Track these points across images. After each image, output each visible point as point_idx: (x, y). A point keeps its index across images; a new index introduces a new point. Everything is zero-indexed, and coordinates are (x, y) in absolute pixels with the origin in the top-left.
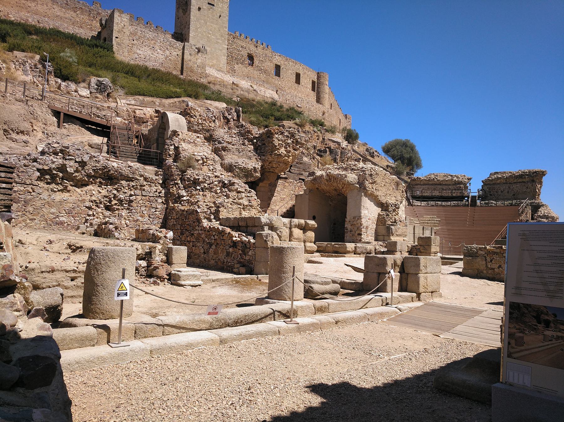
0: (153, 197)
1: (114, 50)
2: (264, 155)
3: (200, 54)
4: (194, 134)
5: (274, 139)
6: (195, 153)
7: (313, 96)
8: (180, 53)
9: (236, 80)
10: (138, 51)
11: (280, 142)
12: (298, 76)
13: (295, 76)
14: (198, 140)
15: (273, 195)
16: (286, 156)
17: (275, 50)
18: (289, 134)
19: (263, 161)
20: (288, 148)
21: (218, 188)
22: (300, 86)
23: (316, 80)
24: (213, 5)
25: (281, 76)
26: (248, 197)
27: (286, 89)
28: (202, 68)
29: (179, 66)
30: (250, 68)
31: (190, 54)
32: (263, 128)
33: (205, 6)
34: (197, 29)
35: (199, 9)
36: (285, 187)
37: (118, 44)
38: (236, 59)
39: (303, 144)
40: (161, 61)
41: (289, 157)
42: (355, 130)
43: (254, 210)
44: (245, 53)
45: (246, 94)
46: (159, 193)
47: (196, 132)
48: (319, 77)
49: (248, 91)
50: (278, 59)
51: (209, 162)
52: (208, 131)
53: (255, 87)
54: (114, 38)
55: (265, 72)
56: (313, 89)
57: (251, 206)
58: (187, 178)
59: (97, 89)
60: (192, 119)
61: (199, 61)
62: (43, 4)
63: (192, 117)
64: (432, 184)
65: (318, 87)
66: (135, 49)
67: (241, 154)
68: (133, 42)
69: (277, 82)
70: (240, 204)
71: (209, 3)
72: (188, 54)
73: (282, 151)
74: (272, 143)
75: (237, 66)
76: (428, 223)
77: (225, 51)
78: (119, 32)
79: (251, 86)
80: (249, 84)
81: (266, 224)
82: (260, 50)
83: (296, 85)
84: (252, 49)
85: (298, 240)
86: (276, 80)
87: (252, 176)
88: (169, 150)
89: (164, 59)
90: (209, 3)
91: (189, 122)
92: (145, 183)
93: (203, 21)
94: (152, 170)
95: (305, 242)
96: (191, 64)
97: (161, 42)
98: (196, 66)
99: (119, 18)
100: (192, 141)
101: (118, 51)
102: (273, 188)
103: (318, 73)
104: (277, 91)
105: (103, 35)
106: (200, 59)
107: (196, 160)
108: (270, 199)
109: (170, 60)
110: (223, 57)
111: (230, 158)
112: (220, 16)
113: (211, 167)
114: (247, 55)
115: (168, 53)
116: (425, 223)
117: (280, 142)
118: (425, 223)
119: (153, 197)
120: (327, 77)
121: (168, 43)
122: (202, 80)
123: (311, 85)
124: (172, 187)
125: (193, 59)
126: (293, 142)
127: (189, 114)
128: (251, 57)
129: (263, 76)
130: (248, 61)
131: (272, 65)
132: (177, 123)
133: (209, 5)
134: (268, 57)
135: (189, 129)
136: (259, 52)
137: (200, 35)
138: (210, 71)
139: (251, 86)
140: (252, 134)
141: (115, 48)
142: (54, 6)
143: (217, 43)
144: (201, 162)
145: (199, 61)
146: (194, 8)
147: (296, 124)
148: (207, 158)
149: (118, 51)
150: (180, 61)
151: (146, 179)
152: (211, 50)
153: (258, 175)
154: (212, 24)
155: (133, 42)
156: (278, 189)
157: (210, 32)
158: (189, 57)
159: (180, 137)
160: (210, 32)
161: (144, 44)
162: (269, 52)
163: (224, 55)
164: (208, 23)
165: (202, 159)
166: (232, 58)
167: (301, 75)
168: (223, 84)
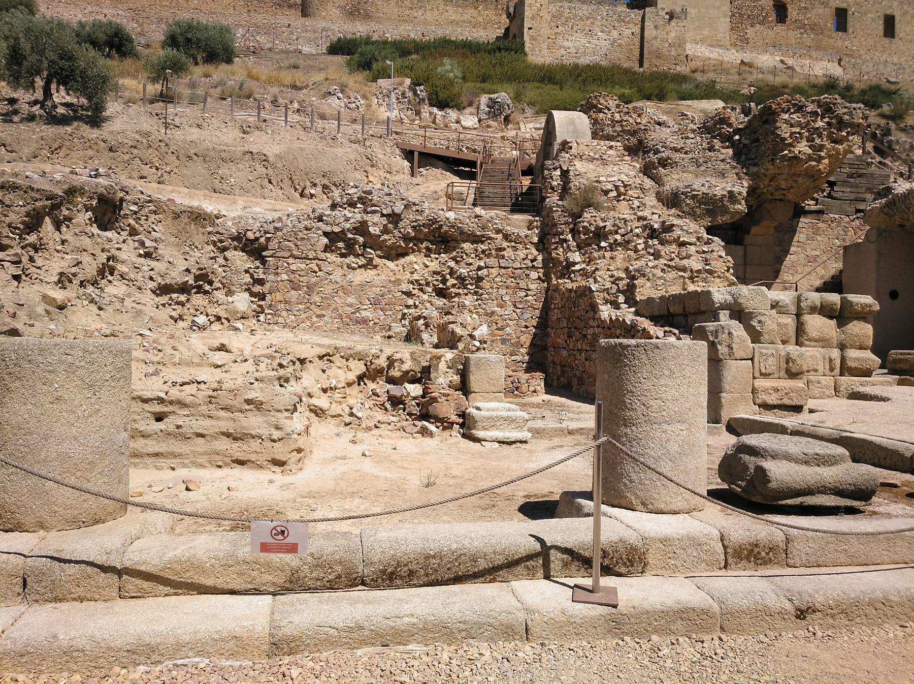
0: (521, 268)
1: (526, 49)
2: (755, 165)
3: (673, 23)
4: (602, 143)
5: (778, 124)
6: (602, 179)
8: (637, 30)
9: (747, 57)
10: (566, 44)
11: (794, 130)
13: (882, 22)
14: (610, 152)
15: (786, 252)
16: (810, 158)
18: (819, 106)
19: (754, 177)
20: (818, 141)
21: (641, 241)
22: (894, 41)
25: (850, 30)
26: (704, 252)
27: (862, 52)
28: (679, 46)
29: (637, 53)
30: (780, 28)
31: (656, 27)
36: (817, 231)
37: (533, 38)
38: (749, 17)
39: (859, 125)
40: (604, 51)
41: (819, 160)
43: (717, 280)
45: (770, 78)
46: (532, 261)
47: (609, 138)
49: (774, 71)
51: (630, 192)
52: (633, 133)
53: (790, 62)
54: (526, 30)
55: (813, 28)
57: (710, 272)
58: (584, 227)
59: (489, 112)
60: (601, 115)
61: (673, 34)
62: (432, 9)
63: (600, 111)
66: (560, 41)
67: (703, 168)
69: (839, 43)
70: (684, 269)
72: (652, 26)
73: (803, 148)
74: (773, 133)
75: (752, 29)
78: (533, 18)
79: (782, 62)
80: (778, 58)
81: (723, 307)
83: (886, 41)
85: (824, 342)
86: (840, 41)
87: (724, 210)
88: (551, 178)
89: (609, 47)
91: (595, 122)
92: (505, 244)
94: (522, 221)
95: (842, 347)
96: (656, 44)
97: (602, 18)
98: (667, 45)
100: (597, 156)
102: (786, 237)
104: (840, 61)
105: (513, 31)
106: (674, 31)
107: (602, 191)
108: (780, 260)
109: (620, 45)
110: (722, 20)
111: (674, 180)
113: (637, 203)
115: (615, 33)
117: (794, 130)
119: (521, 268)
121: (615, 17)
122: (678, 68)
124: (556, 249)
125: (661, 33)
126: (829, 124)
127: (595, 107)
129: (808, 38)
130: (773, 17)
132: (572, 127)
135: (595, 135)
138: (691, 49)
139: (782, 62)
140: (730, 125)
141: (528, 45)
142: (448, 8)
144: (614, 194)
145: (673, 34)
147: (883, 116)
148: (625, 186)
149: (533, 50)
150: (638, 44)
151: (506, 237)
153: (742, 207)
156: (800, 236)
158: (654, 32)
159: (573, 151)
161: (575, 28)
163: (725, 16)
165: (617, 187)
168: (720, 67)
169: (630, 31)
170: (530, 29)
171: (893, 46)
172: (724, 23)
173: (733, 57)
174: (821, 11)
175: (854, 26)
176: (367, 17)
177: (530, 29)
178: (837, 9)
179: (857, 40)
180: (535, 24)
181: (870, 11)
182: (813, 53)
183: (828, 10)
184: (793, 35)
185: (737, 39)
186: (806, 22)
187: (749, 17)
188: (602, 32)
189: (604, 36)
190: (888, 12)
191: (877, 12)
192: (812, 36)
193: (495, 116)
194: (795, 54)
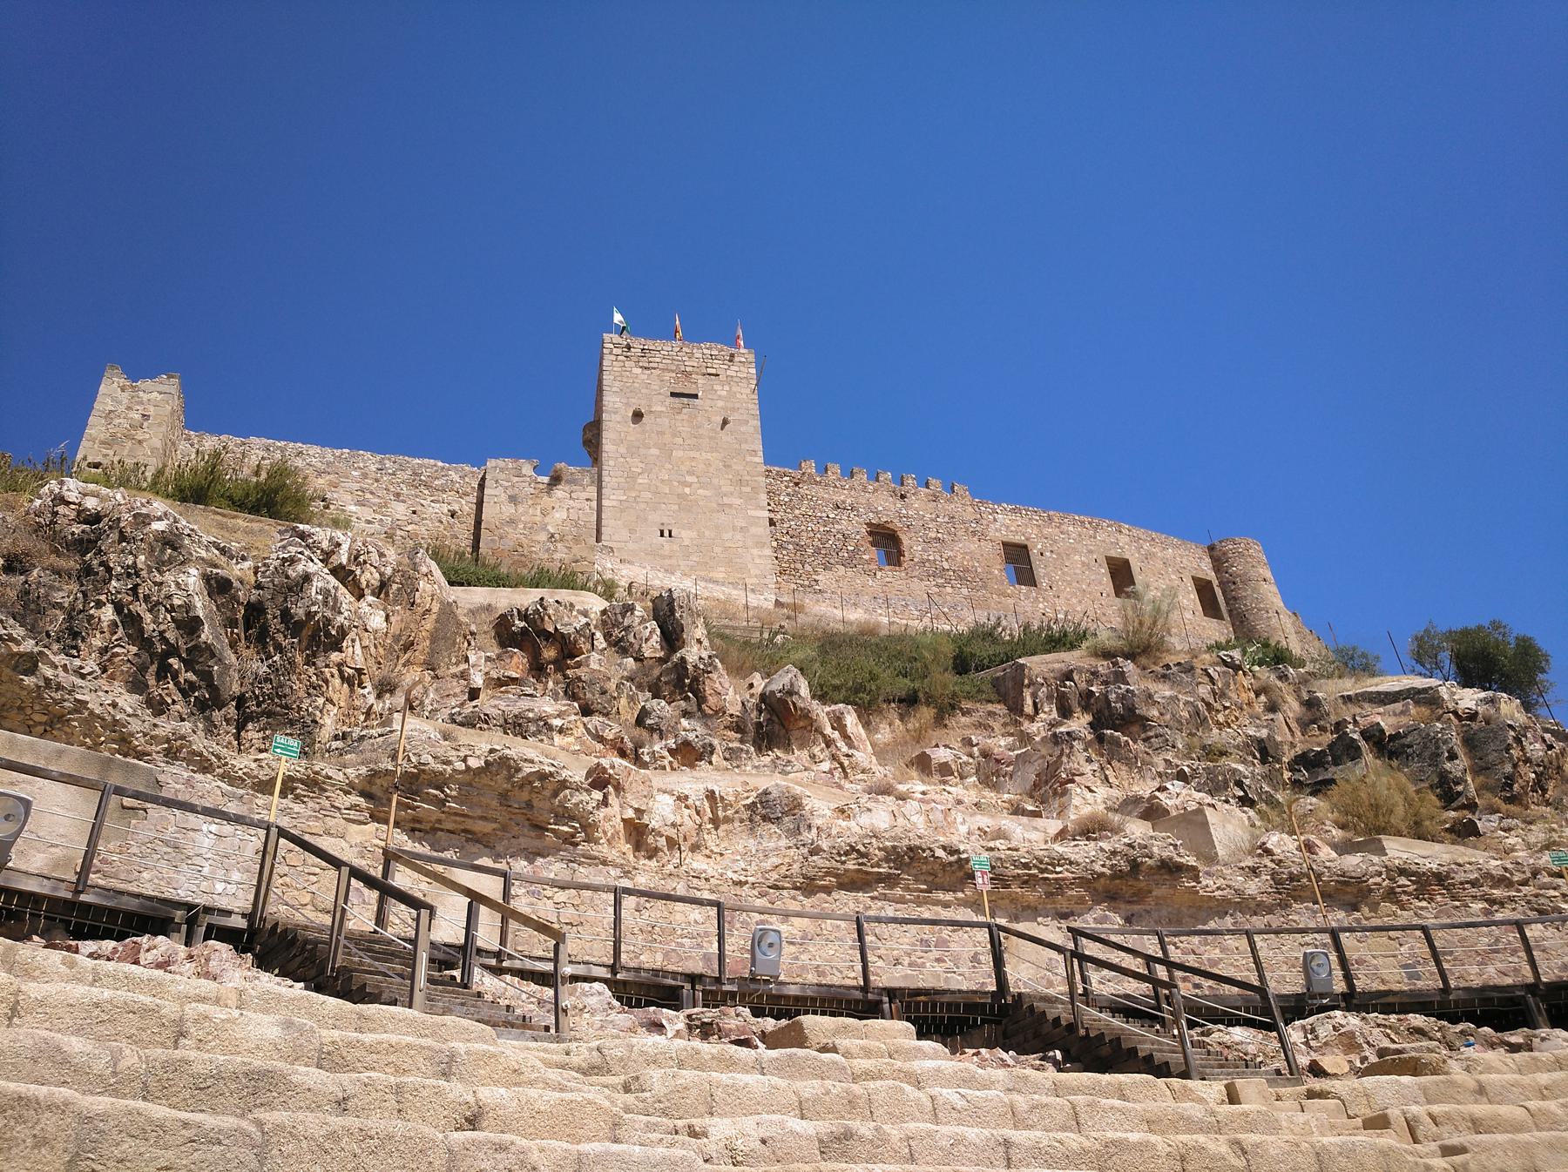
3: (560, 492)
8: (467, 506)
17: (986, 492)
23: (1211, 576)
24: (696, 396)
30: (888, 574)
31: (513, 499)
32: (892, 712)
33: (661, 405)
34: (632, 477)
35: (638, 416)
38: (817, 551)
42: (1496, 625)
44: (855, 527)
48: (1219, 561)
50: (1008, 523)
55: (963, 576)
56: (1210, 606)
71: (673, 394)
72: (504, 497)
75: (829, 574)
77: (763, 530)
84: (884, 506)
90: (673, 394)
93: (654, 451)
96: (514, 535)
97: (365, 476)
98: (543, 537)
99: (125, 397)
103: (1211, 548)
110: (755, 552)
112: (725, 422)
114: (864, 530)
115: (400, 510)
120: (1256, 551)
123: (1194, 596)
125: (528, 513)
128: (887, 541)
130: (871, 553)
131: (987, 547)
133: (677, 400)
136: (917, 511)
137: (647, 495)
143: (723, 507)
145: (560, 515)
146: (618, 418)
152: (701, 535)
154: (692, 454)
157: (689, 479)
158: (509, 510)
160: (689, 479)
162: (962, 505)
163: (761, 545)
164: (677, 454)
166: (796, 556)
167: (1135, 566)
169: (445, 509)
178: (1004, 544)
179: (1062, 601)
181: (1075, 551)
183: (987, 547)
188: (360, 503)
189: (367, 513)
190: (1113, 554)
192: (965, 591)
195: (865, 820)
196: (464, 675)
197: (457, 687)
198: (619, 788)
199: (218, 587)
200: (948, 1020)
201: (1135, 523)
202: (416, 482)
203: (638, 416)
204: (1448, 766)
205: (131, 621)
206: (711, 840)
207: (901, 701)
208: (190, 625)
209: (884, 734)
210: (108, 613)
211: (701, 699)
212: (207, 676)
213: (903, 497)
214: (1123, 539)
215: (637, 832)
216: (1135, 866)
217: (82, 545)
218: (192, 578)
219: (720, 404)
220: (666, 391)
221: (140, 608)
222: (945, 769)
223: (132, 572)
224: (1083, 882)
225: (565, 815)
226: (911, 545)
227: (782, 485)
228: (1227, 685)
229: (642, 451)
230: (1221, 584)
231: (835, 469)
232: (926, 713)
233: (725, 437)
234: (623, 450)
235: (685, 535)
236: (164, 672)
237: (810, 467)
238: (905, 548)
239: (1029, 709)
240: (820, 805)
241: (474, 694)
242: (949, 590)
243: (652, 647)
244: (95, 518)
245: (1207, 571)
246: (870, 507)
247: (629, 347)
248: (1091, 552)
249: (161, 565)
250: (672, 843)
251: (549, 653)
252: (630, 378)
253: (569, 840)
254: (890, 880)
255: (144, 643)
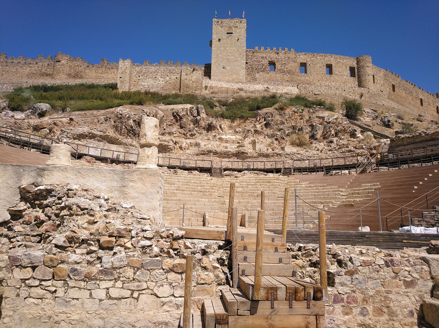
1: (118, 87)
3: (195, 72)
7: (353, 82)
8: (178, 76)
10: (143, 84)
12: (329, 67)
17: (299, 50)
22: (332, 76)
23: (356, 66)
24: (232, 33)
27: (315, 82)
28: (197, 82)
30: (272, 74)
31: (186, 74)
33: (225, 36)
35: (219, 40)
38: (256, 69)
40: (162, 86)
44: (265, 62)
48: (358, 63)
50: (302, 58)
55: (289, 72)
59: (32, 112)
61: (194, 77)
62: (111, 73)
64: (421, 142)
65: (358, 72)
66: (140, 83)
68: (139, 78)
69: (303, 78)
71: (227, 33)
72: (185, 74)
76: (359, 194)
77: (244, 65)
80: (266, 86)
82: (282, 55)
83: (328, 76)
84: (273, 56)
86: (303, 77)
90: (227, 33)
93: (223, 48)
96: (186, 82)
98: (191, 82)
101: (121, 87)
103: (357, 58)
104: (298, 86)
109: (170, 83)
110: (242, 71)
112: (238, 39)
115: (168, 78)
116: (355, 193)
118: (355, 193)
125: (189, 77)
129: (287, 77)
130: (268, 68)
134: (289, 58)
136: (281, 56)
143: (236, 61)
145: (194, 77)
146: (215, 41)
147: (276, 109)
150: (179, 82)
152: (231, 68)
154: (231, 48)
155: (139, 78)
157: (230, 54)
158: (186, 77)
160: (230, 54)
161: (148, 77)
162: (292, 55)
163: (243, 69)
164: (227, 48)
166: (252, 70)
168: (227, 91)
169: (175, 77)
170: (121, 78)
171: (332, 78)
172: (243, 72)
173: (259, 87)
174: (293, 65)
175: (310, 70)
176: (81, 77)
177: (121, 78)
180: (123, 76)
181: (319, 63)
182: (284, 83)
184: (279, 76)
185: (251, 79)
186: (285, 70)
187: (256, 69)
188: (161, 78)
189: (162, 79)
190: (328, 63)
191: (322, 63)
192: (289, 76)
193: (34, 113)
194: (275, 84)
195: (207, 146)
196: (163, 127)
197: (163, 129)
198: (178, 143)
199: (134, 121)
200: (202, 170)
201: (337, 54)
202: (170, 72)
203: (219, 40)
204: (315, 132)
205: (126, 127)
206: (190, 148)
207: (239, 117)
208: (132, 127)
209: (235, 124)
210: (124, 127)
211: (199, 125)
212: (134, 132)
213: (278, 53)
214: (332, 59)
215: (181, 148)
216: (239, 152)
217: (121, 118)
218: (131, 121)
219: (238, 34)
220: (226, 33)
221: (127, 126)
222: (237, 132)
223: (125, 122)
224: (232, 154)
225: (168, 148)
226: (278, 66)
227: (250, 54)
228: (292, 116)
229: (220, 49)
230: (358, 68)
231: (263, 48)
232: (242, 121)
233: (238, 43)
234: (216, 49)
235: (228, 68)
236: (130, 132)
237: (257, 48)
238: (276, 67)
239: (258, 120)
240: (202, 144)
241: (165, 129)
242: (285, 76)
243: (196, 114)
244: (121, 115)
245: (355, 65)
246: (270, 57)
247: (218, 22)
248: (322, 63)
249: (128, 120)
250: (185, 149)
251: (178, 118)
252: (218, 30)
253: (169, 151)
254: (207, 154)
255: (128, 130)
